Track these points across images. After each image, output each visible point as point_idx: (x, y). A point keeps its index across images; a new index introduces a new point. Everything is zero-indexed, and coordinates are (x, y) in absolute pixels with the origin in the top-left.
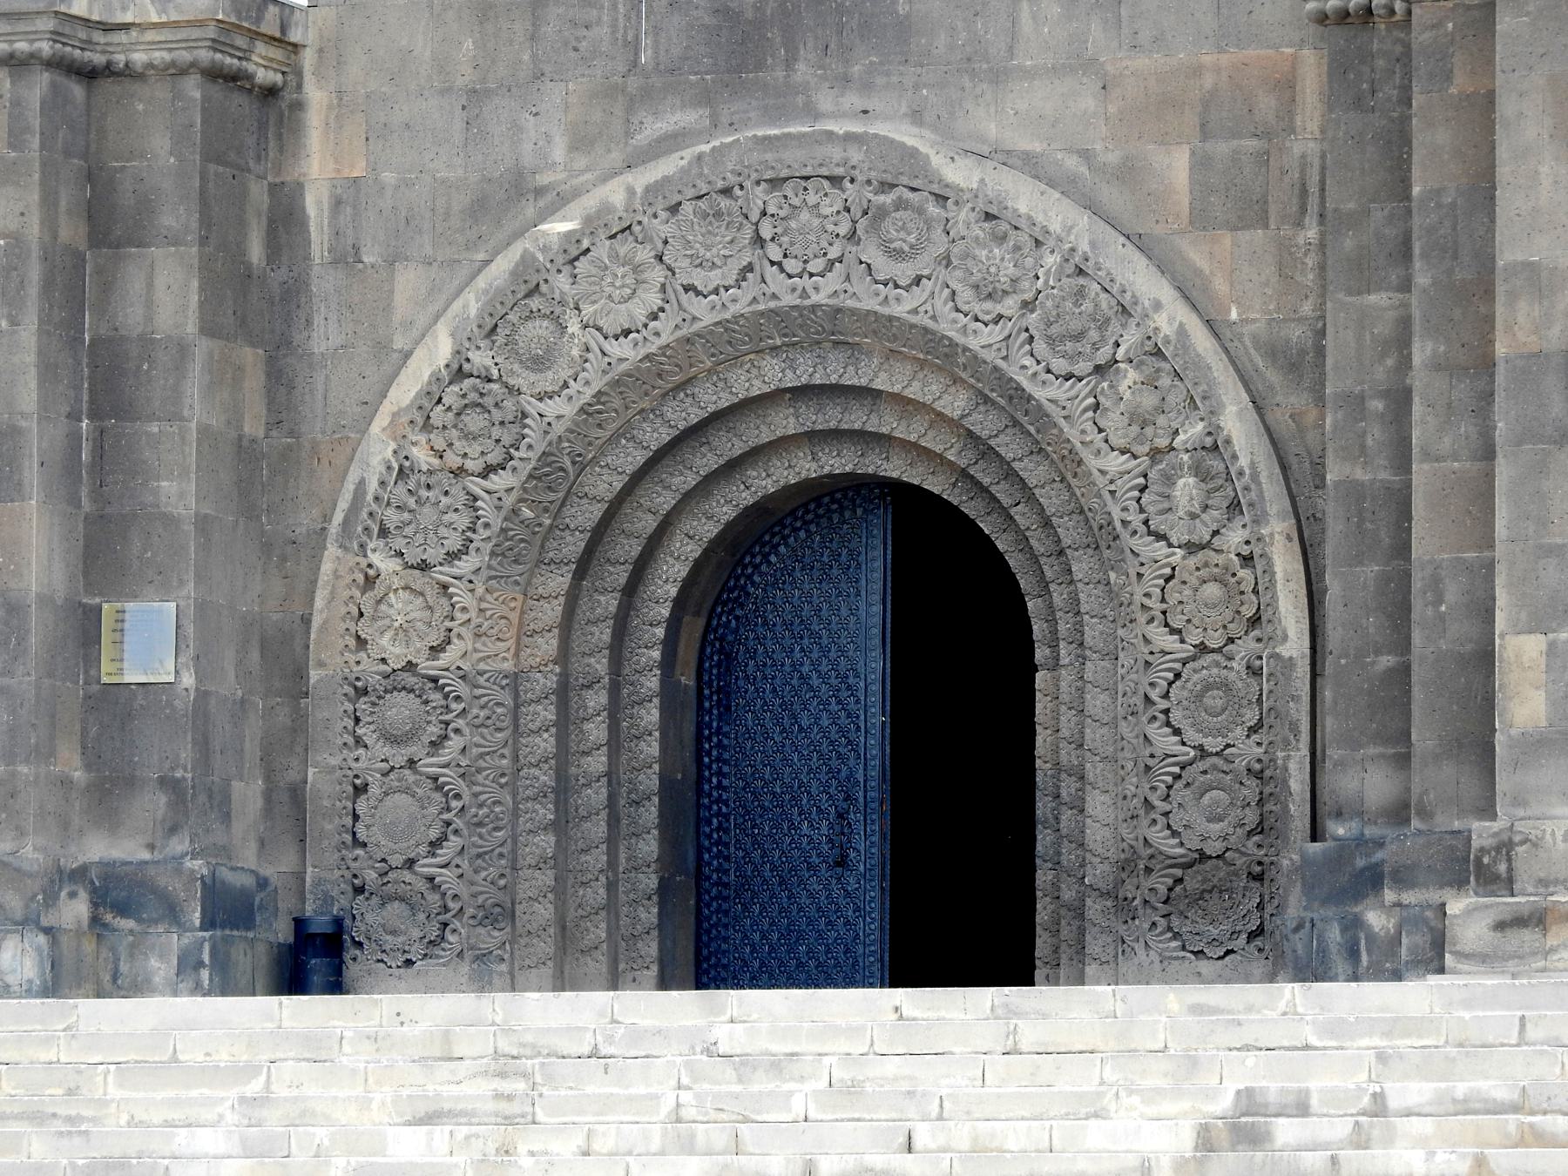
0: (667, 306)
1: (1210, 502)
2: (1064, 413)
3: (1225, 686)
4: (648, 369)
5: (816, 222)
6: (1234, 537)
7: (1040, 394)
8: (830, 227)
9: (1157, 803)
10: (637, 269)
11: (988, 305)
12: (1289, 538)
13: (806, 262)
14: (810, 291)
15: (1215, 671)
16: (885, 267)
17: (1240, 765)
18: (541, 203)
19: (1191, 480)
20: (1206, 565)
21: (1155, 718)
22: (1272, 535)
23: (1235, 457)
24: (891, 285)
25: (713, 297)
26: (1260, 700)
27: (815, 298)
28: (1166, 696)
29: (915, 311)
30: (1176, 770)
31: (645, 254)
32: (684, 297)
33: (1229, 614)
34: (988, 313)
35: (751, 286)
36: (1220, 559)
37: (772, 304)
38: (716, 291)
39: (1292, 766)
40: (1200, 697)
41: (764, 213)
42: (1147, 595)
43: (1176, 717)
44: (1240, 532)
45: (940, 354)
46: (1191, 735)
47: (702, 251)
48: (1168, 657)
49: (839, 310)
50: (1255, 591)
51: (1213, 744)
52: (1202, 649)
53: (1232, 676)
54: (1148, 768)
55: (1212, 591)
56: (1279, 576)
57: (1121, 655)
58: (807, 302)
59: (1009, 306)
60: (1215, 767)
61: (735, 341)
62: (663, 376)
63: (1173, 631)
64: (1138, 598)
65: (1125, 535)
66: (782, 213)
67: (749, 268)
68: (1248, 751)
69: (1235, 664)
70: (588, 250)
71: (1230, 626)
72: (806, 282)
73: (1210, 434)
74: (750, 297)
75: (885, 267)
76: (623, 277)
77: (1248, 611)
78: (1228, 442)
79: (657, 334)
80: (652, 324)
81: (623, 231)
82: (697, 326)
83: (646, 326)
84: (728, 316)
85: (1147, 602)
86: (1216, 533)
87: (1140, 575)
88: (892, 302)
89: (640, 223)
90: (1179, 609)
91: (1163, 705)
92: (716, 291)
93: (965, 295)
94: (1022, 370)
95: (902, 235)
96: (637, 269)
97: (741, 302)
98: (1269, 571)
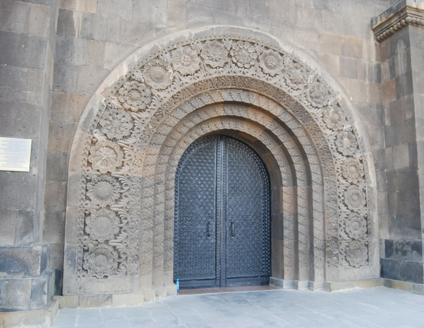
0: (201, 70)
1: (352, 145)
2: (316, 117)
3: (358, 195)
4: (193, 87)
5: (247, 54)
6: (358, 156)
7: (309, 111)
8: (251, 56)
9: (342, 225)
10: (192, 57)
11: (295, 85)
12: (371, 157)
13: (244, 64)
14: (245, 73)
15: (355, 190)
16: (266, 70)
17: (362, 215)
18: (158, 33)
19: (347, 139)
20: (352, 162)
21: (341, 202)
22: (367, 155)
23: (358, 134)
24: (268, 75)
25: (215, 69)
26: (366, 198)
27: (247, 75)
28: (343, 196)
29: (275, 83)
30: (346, 216)
31: (195, 53)
32: (207, 68)
33: (357, 175)
34: (295, 87)
35: (227, 69)
36: (355, 161)
37: (234, 74)
38: (216, 68)
39: (374, 216)
40: (351, 196)
41: (231, 48)
42: (338, 168)
43: (346, 202)
44: (360, 154)
45: (278, 96)
46: (350, 207)
47: (212, 56)
48: (344, 185)
49: (253, 80)
50: (363, 170)
51: (355, 210)
52: (352, 184)
53: (359, 192)
54: (340, 215)
55: (353, 168)
56: (369, 166)
57: (326, 184)
58: (245, 76)
59: (301, 86)
60: (356, 216)
61: (219, 84)
62: (196, 90)
63: (344, 178)
64: (336, 169)
65: (332, 152)
66: (237, 49)
67: (227, 63)
68: (363, 212)
69: (359, 188)
70: (175, 49)
71: (358, 178)
72: (243, 70)
73: (351, 128)
74: (227, 71)
75: (266, 70)
76: (187, 59)
77: (362, 175)
78: (356, 130)
79: (198, 77)
80: (196, 74)
81: (187, 45)
82: (210, 77)
83: (194, 74)
84: (221, 75)
85: (338, 170)
86: (354, 153)
87: (336, 163)
88: (269, 80)
89: (193, 44)
90: (346, 172)
91: (343, 198)
92: (216, 68)
93: (288, 81)
94: (305, 104)
95: (272, 62)
96: (192, 57)
97: (225, 72)
98: (367, 164)
